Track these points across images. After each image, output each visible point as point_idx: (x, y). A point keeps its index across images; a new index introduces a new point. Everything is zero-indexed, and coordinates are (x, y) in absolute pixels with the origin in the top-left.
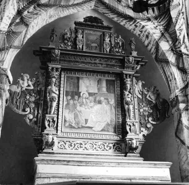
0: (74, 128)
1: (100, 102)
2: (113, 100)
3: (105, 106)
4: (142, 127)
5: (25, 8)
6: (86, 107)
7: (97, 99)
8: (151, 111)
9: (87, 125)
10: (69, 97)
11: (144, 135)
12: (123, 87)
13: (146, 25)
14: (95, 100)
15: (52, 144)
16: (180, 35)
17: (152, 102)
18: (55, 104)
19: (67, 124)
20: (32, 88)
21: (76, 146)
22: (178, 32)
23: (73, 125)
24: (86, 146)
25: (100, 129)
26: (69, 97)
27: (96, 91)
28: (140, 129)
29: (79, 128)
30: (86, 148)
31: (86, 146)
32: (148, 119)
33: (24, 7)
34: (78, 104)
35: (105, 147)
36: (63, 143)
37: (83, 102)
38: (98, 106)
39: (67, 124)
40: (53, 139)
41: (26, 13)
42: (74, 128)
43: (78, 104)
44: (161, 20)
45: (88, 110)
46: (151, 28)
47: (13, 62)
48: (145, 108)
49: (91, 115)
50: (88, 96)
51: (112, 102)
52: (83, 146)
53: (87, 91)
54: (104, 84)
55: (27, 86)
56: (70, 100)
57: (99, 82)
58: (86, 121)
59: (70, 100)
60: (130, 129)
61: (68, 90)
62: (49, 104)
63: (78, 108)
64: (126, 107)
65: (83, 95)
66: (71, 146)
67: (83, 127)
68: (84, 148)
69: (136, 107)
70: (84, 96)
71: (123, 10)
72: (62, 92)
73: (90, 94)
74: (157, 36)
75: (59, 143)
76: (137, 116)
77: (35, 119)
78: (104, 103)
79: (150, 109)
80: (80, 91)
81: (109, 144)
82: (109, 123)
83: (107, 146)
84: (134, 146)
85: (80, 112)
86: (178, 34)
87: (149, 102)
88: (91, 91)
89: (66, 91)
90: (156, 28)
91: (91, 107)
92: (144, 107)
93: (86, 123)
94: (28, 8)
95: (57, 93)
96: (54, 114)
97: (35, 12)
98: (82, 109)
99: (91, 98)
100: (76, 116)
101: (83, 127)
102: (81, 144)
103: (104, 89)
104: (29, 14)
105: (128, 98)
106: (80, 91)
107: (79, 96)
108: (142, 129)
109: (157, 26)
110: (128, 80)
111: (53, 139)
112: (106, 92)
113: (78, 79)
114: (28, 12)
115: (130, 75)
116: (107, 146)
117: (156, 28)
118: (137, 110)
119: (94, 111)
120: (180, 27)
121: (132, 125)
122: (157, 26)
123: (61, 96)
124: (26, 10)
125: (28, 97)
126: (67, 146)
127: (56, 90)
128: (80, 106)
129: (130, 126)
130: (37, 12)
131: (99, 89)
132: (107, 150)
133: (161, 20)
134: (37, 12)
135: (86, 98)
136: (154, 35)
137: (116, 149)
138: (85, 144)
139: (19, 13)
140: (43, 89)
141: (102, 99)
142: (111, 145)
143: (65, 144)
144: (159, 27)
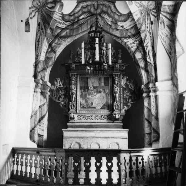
0: (85, 108)
1: (100, 92)
2: (108, 90)
3: (103, 94)
4: (124, 105)
5: (53, 41)
6: (92, 96)
7: (98, 90)
8: (131, 95)
9: (93, 106)
10: (83, 90)
11: (125, 110)
12: (113, 82)
13: (127, 42)
14: (97, 91)
15: (74, 118)
16: (146, 50)
17: (132, 90)
18: (74, 96)
19: (82, 106)
20: (62, 86)
21: (87, 118)
22: (145, 47)
23: (85, 106)
24: (92, 118)
25: (100, 108)
26: (83, 90)
27: (98, 85)
28: (123, 107)
29: (88, 108)
30: (92, 119)
31: (92, 118)
32: (128, 101)
33: (52, 40)
34: (88, 94)
35: (103, 118)
36: (80, 116)
37: (90, 93)
38: (99, 95)
39: (82, 106)
40: (74, 116)
41: (54, 44)
42: (85, 108)
43: (88, 94)
44: (138, 36)
45: (93, 97)
46: (130, 43)
47: (48, 118)
48: (127, 94)
49: (95, 100)
50: (93, 88)
51: (107, 91)
52: (90, 118)
53: (93, 86)
54: (103, 81)
55: (59, 86)
56: (83, 92)
57: (100, 79)
58: (92, 103)
59: (83, 92)
60: (116, 108)
61: (82, 86)
62: (71, 96)
63: (88, 96)
64: (115, 94)
65: (90, 88)
66: (84, 118)
67: (90, 107)
68: (91, 119)
69: (121, 94)
70: (91, 89)
71: (112, 32)
72: (78, 88)
73: (94, 88)
74: (134, 49)
75: (78, 116)
76: (122, 99)
77: (65, 104)
78: (102, 92)
79: (130, 94)
80: (88, 86)
81: (104, 116)
82: (105, 104)
83: (103, 118)
84: (117, 117)
85: (89, 98)
86: (146, 49)
87: (130, 90)
88: (95, 86)
89: (81, 87)
90: (134, 43)
91: (95, 95)
92: (126, 93)
93: (92, 105)
94: (54, 41)
95: (75, 90)
96: (74, 102)
97: (59, 43)
98: (90, 97)
99: (95, 90)
100: (86, 101)
101: (90, 107)
102: (89, 117)
103: (103, 84)
104: (55, 44)
105: (116, 89)
106: (88, 86)
107: (88, 89)
108: (124, 106)
109: (134, 42)
110: (116, 78)
111: (74, 116)
112: (104, 86)
113: (87, 78)
114: (55, 43)
115: (117, 75)
116: (103, 118)
117: (134, 43)
118: (122, 96)
119: (97, 98)
120: (147, 45)
121: (117, 106)
122: (134, 42)
123: (78, 90)
124: (53, 42)
125: (60, 92)
126: (82, 118)
127: (74, 88)
128: (89, 95)
129: (116, 106)
130: (60, 42)
131: (99, 84)
132: (103, 119)
133: (138, 36)
134: (60, 42)
135: (92, 90)
136: (132, 49)
137: (108, 119)
138: (92, 117)
139: (50, 45)
140: (68, 86)
141: (101, 90)
142: (105, 117)
143: (81, 117)
144: (135, 42)
